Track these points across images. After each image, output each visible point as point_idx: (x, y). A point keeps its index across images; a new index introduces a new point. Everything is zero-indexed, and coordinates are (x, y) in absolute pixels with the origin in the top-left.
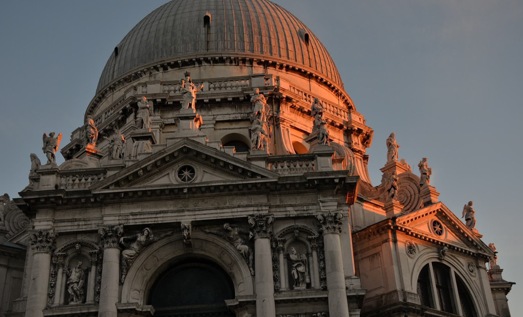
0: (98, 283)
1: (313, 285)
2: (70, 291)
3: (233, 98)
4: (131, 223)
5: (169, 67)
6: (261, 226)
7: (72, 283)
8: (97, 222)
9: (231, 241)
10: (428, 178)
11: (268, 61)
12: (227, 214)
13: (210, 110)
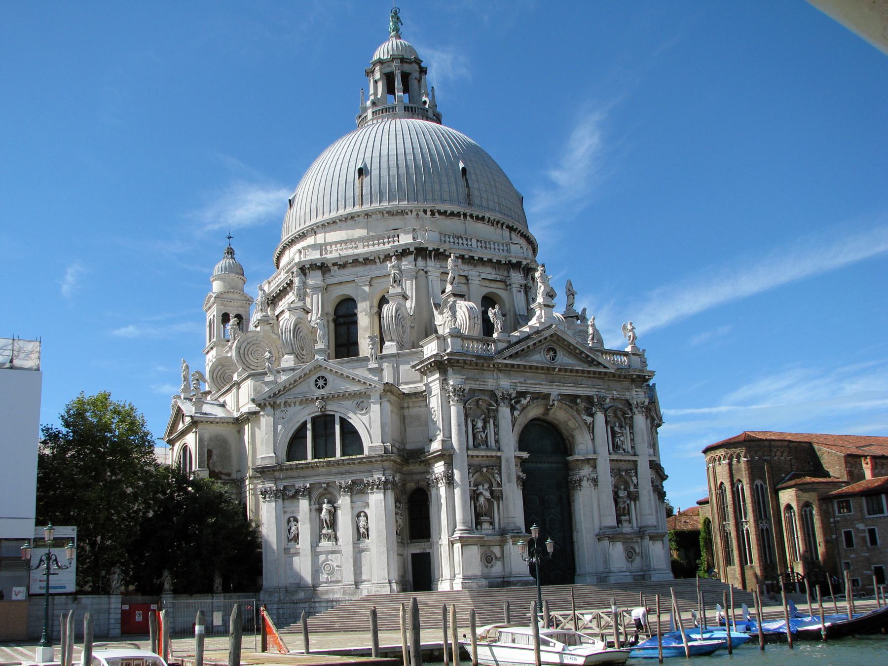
0: (496, 434)
1: (626, 450)
2: (480, 438)
3: (497, 260)
4: (519, 389)
5: (436, 214)
6: (601, 404)
7: (480, 432)
8: (492, 384)
10: (646, 365)
11: (513, 226)
13: (475, 266)
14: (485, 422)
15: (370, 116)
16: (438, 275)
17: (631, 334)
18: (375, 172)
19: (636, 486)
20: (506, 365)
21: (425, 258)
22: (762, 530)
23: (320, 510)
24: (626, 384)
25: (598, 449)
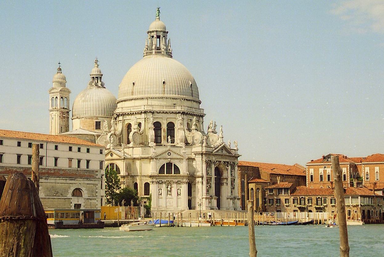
9: (225, 165)
12: (227, 160)
14: (209, 168)
15: (154, 53)
16: (186, 120)
17: (236, 144)
18: (168, 84)
19: (234, 185)
20: (215, 154)
21: (183, 115)
22: (242, 195)
23: (167, 187)
24: (234, 158)
25: (228, 176)
